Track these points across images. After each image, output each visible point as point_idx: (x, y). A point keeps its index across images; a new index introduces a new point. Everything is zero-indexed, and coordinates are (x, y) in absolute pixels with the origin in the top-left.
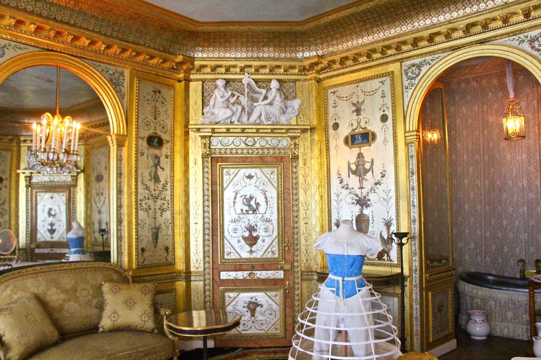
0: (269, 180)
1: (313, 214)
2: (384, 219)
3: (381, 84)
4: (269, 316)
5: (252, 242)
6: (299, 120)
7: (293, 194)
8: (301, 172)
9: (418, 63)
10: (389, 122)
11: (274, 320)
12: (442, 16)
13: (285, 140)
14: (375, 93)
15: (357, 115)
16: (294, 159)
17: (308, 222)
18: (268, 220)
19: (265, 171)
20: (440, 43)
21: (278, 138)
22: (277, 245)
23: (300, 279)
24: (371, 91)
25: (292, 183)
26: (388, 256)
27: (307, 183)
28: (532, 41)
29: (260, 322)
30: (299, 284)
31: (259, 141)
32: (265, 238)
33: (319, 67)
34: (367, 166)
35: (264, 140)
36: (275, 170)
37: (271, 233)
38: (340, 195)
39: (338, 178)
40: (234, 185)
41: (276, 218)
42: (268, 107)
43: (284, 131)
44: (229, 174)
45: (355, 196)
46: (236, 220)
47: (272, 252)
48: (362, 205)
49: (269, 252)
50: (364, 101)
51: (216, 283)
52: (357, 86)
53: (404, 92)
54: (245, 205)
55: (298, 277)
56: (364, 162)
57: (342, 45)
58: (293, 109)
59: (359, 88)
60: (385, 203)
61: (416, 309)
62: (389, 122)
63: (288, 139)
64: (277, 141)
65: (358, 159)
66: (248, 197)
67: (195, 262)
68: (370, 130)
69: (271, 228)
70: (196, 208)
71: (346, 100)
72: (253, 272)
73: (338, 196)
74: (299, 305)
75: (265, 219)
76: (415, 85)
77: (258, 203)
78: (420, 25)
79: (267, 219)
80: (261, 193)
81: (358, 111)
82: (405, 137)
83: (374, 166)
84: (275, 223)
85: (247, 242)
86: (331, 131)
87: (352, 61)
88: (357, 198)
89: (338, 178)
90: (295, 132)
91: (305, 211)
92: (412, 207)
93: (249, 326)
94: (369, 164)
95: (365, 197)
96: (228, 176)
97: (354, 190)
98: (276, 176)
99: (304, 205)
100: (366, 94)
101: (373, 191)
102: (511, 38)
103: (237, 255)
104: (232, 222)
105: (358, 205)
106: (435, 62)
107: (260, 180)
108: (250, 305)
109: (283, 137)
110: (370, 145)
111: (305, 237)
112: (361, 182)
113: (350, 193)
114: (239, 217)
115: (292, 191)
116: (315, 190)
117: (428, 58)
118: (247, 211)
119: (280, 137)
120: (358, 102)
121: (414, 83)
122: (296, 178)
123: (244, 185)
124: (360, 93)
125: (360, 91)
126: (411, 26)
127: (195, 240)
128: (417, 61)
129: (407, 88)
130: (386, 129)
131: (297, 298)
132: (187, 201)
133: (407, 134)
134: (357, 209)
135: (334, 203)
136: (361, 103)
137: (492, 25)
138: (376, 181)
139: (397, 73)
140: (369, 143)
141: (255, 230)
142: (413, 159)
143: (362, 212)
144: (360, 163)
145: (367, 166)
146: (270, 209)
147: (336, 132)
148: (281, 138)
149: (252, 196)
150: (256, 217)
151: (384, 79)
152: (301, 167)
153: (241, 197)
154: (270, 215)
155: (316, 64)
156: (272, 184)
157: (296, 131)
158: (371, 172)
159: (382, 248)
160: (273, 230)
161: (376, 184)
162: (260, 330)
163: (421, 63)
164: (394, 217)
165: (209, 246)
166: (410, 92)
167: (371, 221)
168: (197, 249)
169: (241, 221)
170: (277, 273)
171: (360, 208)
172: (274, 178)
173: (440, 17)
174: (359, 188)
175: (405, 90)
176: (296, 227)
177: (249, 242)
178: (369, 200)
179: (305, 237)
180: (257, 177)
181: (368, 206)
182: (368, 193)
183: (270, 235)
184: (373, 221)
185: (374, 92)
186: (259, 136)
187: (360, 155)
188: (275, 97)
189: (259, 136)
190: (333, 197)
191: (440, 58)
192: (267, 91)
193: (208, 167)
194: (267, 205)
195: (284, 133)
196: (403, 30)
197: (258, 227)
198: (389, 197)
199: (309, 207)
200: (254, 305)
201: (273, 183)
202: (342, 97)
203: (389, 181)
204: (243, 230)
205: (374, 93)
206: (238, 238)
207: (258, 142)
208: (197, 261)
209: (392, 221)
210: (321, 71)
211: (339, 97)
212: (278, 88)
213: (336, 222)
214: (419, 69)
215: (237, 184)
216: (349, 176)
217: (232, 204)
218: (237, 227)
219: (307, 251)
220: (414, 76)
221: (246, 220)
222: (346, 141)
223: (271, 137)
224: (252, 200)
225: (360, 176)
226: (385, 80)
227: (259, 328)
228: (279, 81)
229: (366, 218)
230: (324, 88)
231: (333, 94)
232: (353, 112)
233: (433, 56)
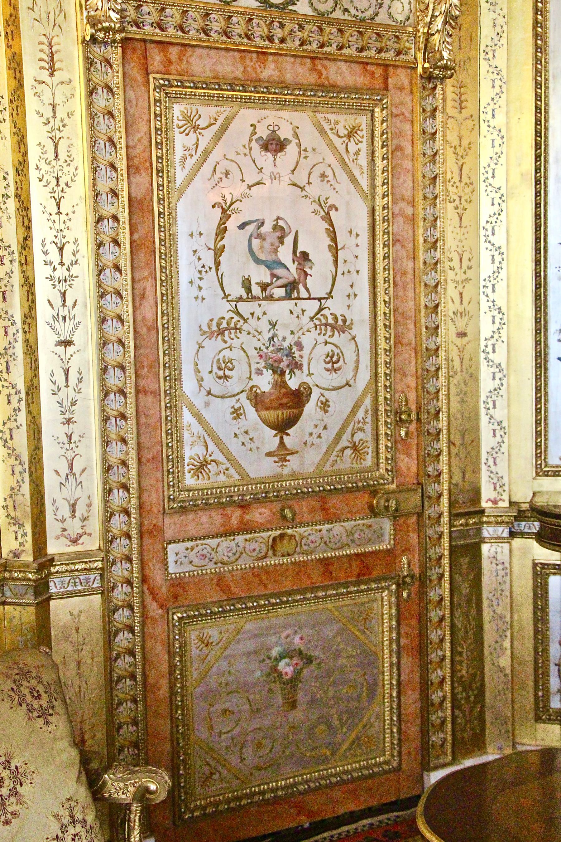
0: (343, 163)
1: (482, 297)
5: (286, 413)
17: (468, 331)
18: (340, 322)
22: (369, 419)
23: (445, 541)
27: (465, 179)
32: (330, 395)
40: (216, 177)
44: (196, 128)
46: (224, 325)
47: (354, 447)
49: (343, 450)
51: (154, 594)
54: (258, 261)
66: (267, 228)
67: (66, 511)
70: (61, 273)
72: (289, 531)
75: (330, 321)
77: (305, 256)
79: (336, 319)
80: (315, 212)
85: (264, 413)
91: (460, 287)
93: (278, 749)
96: (192, 136)
98: (364, 146)
99: (455, 263)
103: (232, 471)
104: (211, 335)
107: (313, 159)
108: (282, 666)
114: (238, 313)
118: (264, 287)
123: (252, 177)
127: (61, 418)
131: (435, 615)
132: (25, 239)
141: (296, 366)
149: (281, 223)
150: (297, 311)
153: (243, 226)
154: (347, 302)
156: (354, 180)
160: (358, 361)
165: (124, 441)
168: (70, 454)
169: (245, 327)
172: (357, 153)
177: (272, 415)
183: (347, 384)
193: (110, 89)
194: (336, 262)
197: (306, 352)
199: (470, 274)
200: (296, 660)
201: (357, 173)
204: (254, 367)
206: (234, 400)
208: (73, 507)
215: (227, 174)
217: (208, 258)
218: (227, 353)
219: (463, 438)
221: (264, 326)
224: (281, 240)
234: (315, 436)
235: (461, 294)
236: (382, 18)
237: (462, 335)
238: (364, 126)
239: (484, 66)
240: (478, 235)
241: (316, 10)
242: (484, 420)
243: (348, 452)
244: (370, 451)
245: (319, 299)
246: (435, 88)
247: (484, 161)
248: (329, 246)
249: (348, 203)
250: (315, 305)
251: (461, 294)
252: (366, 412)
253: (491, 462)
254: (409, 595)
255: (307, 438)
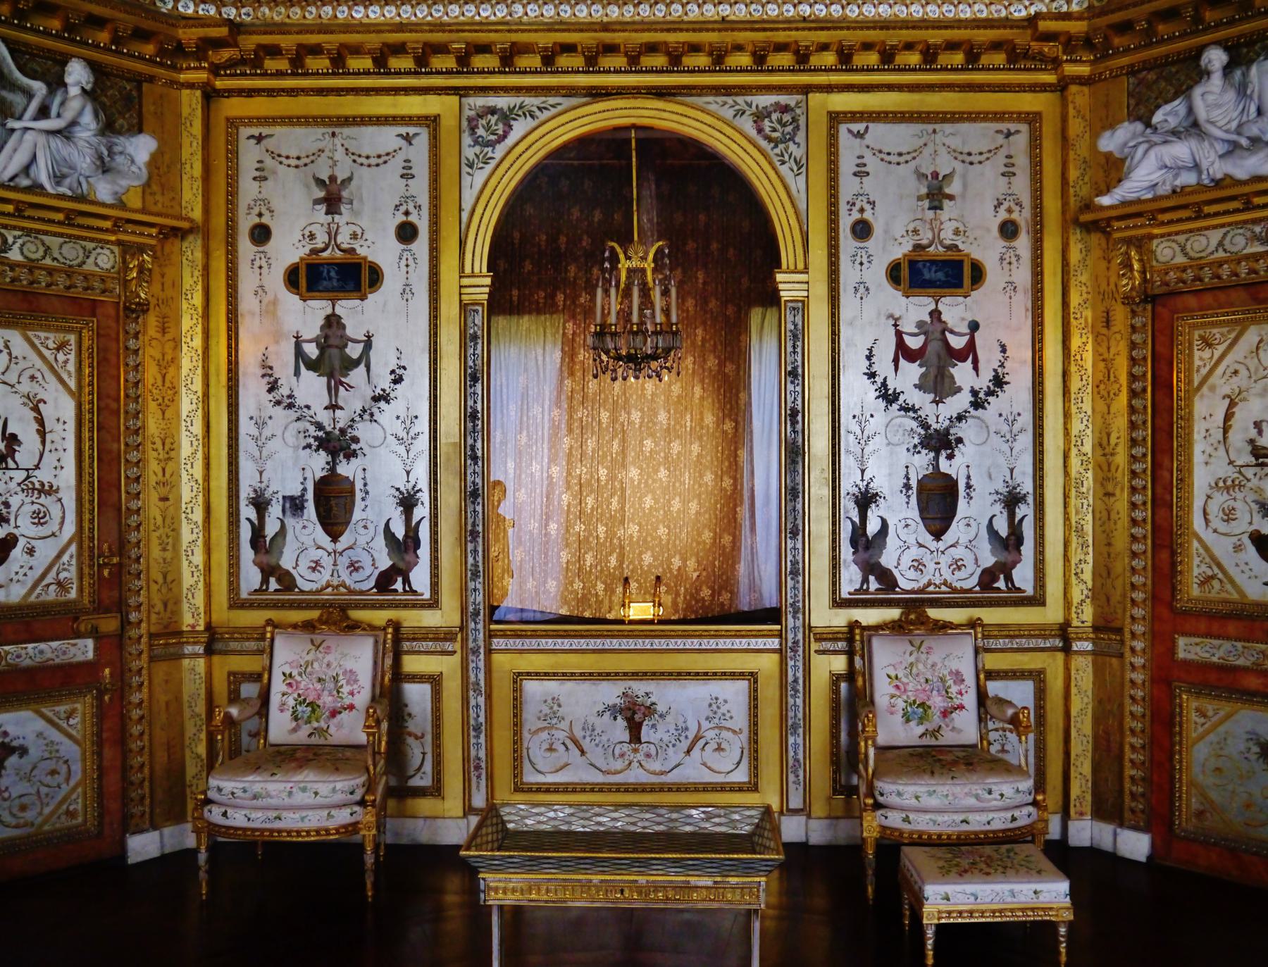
0: (52, 368)
2: (398, 489)
3: (403, 143)
4: (48, 780)
6: (148, 198)
7: (126, 412)
8: (150, 355)
9: (506, 108)
10: (421, 245)
11: (65, 788)
12: (584, 8)
13: (107, 252)
14: (385, 162)
15: (327, 214)
16: (133, 311)
18: (47, 488)
19: (38, 337)
20: (568, 72)
21: (84, 243)
22: (74, 562)
23: (145, 656)
24: (372, 154)
25: (126, 381)
26: (406, 581)
27: (168, 384)
28: (760, 116)
29: (17, 802)
30: (144, 672)
31: (20, 241)
33: (226, 54)
34: (354, 351)
35: (38, 242)
36: (72, 338)
37: (56, 528)
38: (269, 422)
39: (263, 376)
41: (72, 480)
42: (56, 142)
43: (107, 224)
45: (312, 429)
47: (59, 584)
48: (334, 453)
49: (48, 585)
50: (350, 179)
52: (334, 134)
53: (464, 175)
55: (141, 653)
56: (346, 340)
57: (302, 8)
58: (133, 161)
59: (338, 141)
60: (402, 450)
61: (477, 706)
62: (421, 245)
63: (116, 249)
64: (81, 252)
65: (327, 331)
68: (365, 258)
69: (55, 511)
71: (297, 167)
73: (260, 424)
74: (142, 734)
75: (37, 486)
76: (493, 163)
78: (526, 14)
80: (24, 404)
81: (332, 202)
82: (461, 287)
83: (372, 353)
84: (69, 498)
86: (245, 247)
87: (327, 62)
88: (321, 434)
89: (263, 376)
90: (142, 234)
92: (469, 462)
94: (360, 347)
95: (342, 431)
97: (311, 413)
98: (72, 357)
99: (159, 445)
100: (360, 160)
101: (366, 417)
102: (720, 99)
105: (322, 453)
106: (547, 114)
107: (22, 365)
109: (100, 241)
110: (363, 298)
111: (159, 538)
112: (332, 390)
113: (298, 419)
115: (126, 405)
116: (194, 406)
117: (531, 101)
119: (92, 240)
120: (333, 178)
121: (490, 155)
122: (136, 368)
124: (340, 155)
125: (341, 150)
126: (505, 11)
128: (502, 102)
129: (471, 166)
130: (411, 262)
131: (136, 714)
133: (465, 281)
134: (318, 463)
135: (245, 444)
136: (343, 181)
137: (690, 61)
138: (378, 391)
139: (448, 123)
140: (360, 290)
142: (476, 344)
143: (333, 469)
144: (332, 341)
145: (354, 351)
146: (55, 456)
147: (261, 249)
148: (93, 245)
150: (6, 478)
151: (412, 130)
152: (153, 339)
154: (54, 472)
155: (218, 44)
157: (147, 231)
158: (362, 367)
159: (391, 563)
160: (63, 518)
161: (376, 399)
162: (17, 827)
163: (511, 110)
164: (424, 484)
166: (480, 177)
167: (359, 495)
170: (74, 645)
171: (330, 459)
172: (66, 362)
173: (578, 7)
174: (326, 408)
175: (466, 169)
176: (135, 508)
178: (356, 440)
179: (159, 538)
180: (10, 354)
181: (351, 454)
182: (353, 420)
183: (53, 534)
184: (367, 493)
185: (384, 158)
186: (22, 229)
187: (333, 322)
188: (81, 113)
189: (22, 229)
190: (246, 427)
191: (560, 108)
192: (52, 91)
194: (43, 442)
195: (107, 230)
196: (484, 14)
197: (13, 509)
198: (412, 434)
199: (172, 454)
201: (65, 376)
202: (284, 154)
203: (414, 393)
205: (380, 161)
207: (18, 245)
209: (419, 495)
210: (225, 68)
211: (275, 155)
212: (88, 87)
213: (252, 495)
214: (505, 124)
216: (297, 373)
219: (165, 578)
220: (493, 137)
222: (291, 278)
223: (61, 235)
225: (330, 376)
226: (416, 134)
227: (13, 822)
228: (93, 66)
229: (348, 487)
230: (228, 119)
231: (253, 141)
232: (317, 202)
233: (544, 99)
234: (21, 574)
235: (164, 470)
236: (89, 266)
237: (165, 499)
238: (73, 342)
239: (185, 305)
240: (179, 425)
241: (26, 257)
242: (185, 563)
243: (53, 588)
244: (75, 586)
245: (27, 470)
246: (138, 317)
247: (184, 371)
248: (38, 431)
249: (56, 399)
250: (24, 474)
251: (164, 470)
252: (71, 557)
253: (190, 596)
254: (110, 699)
255: (13, 575)
